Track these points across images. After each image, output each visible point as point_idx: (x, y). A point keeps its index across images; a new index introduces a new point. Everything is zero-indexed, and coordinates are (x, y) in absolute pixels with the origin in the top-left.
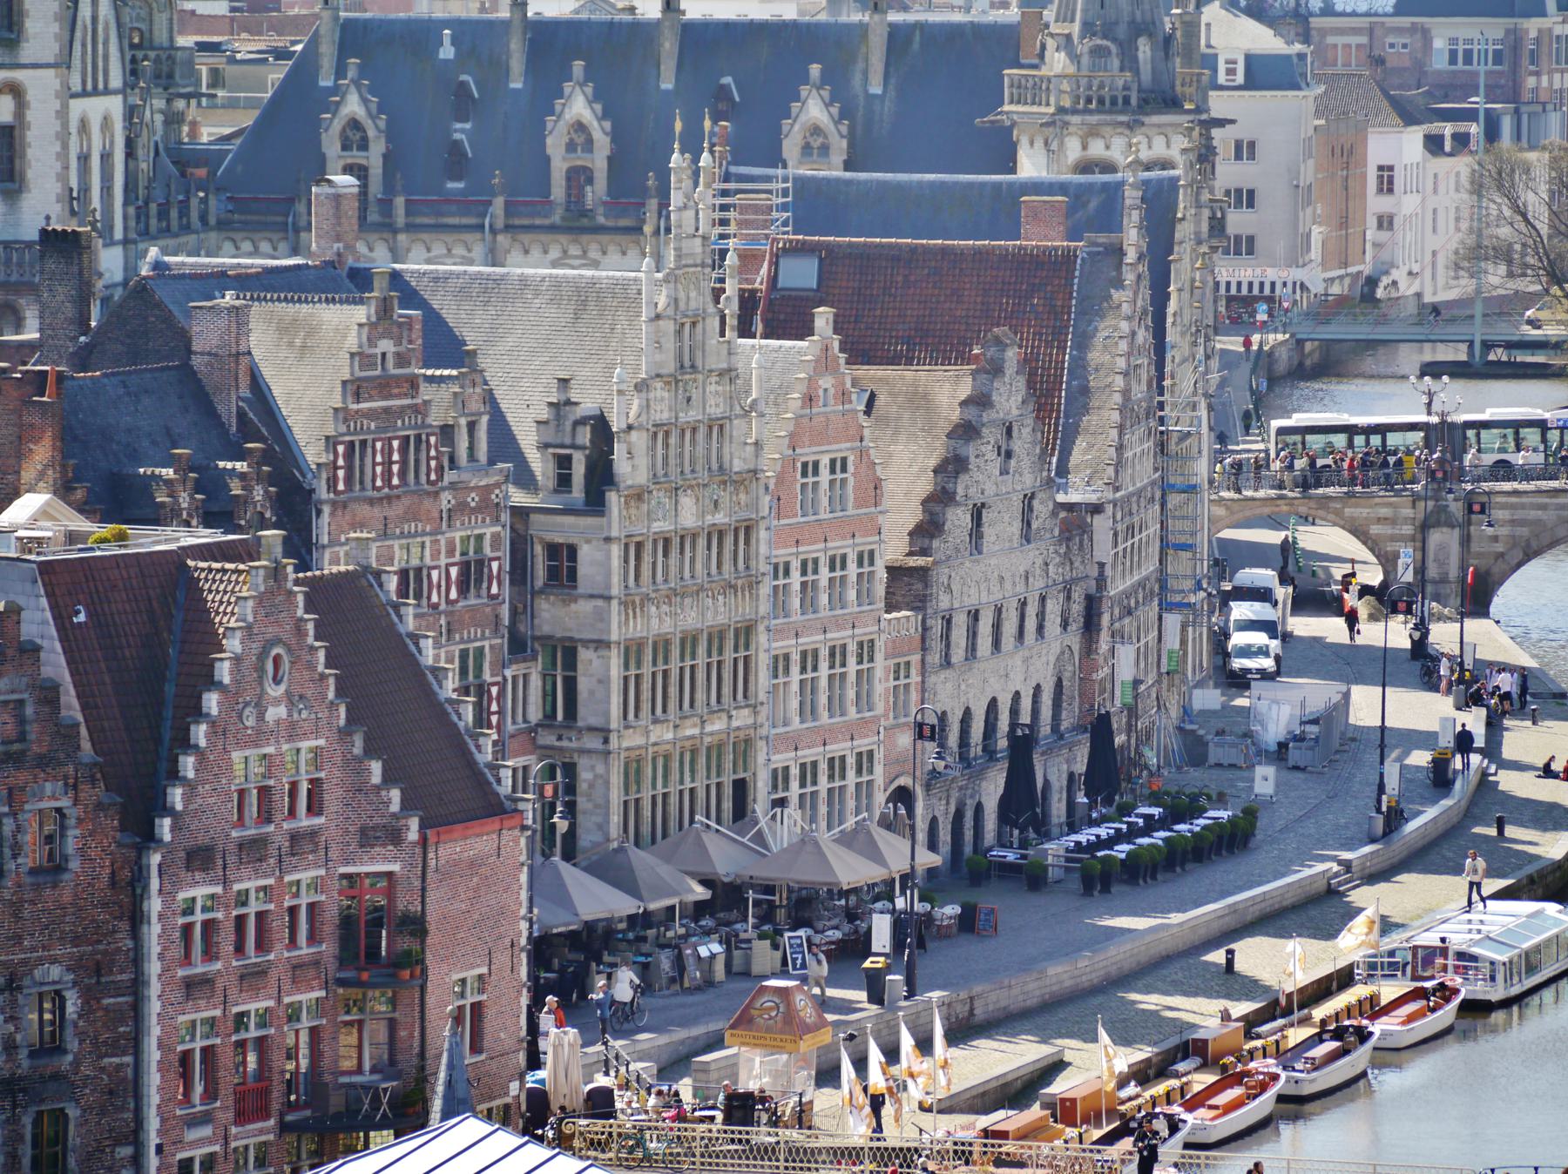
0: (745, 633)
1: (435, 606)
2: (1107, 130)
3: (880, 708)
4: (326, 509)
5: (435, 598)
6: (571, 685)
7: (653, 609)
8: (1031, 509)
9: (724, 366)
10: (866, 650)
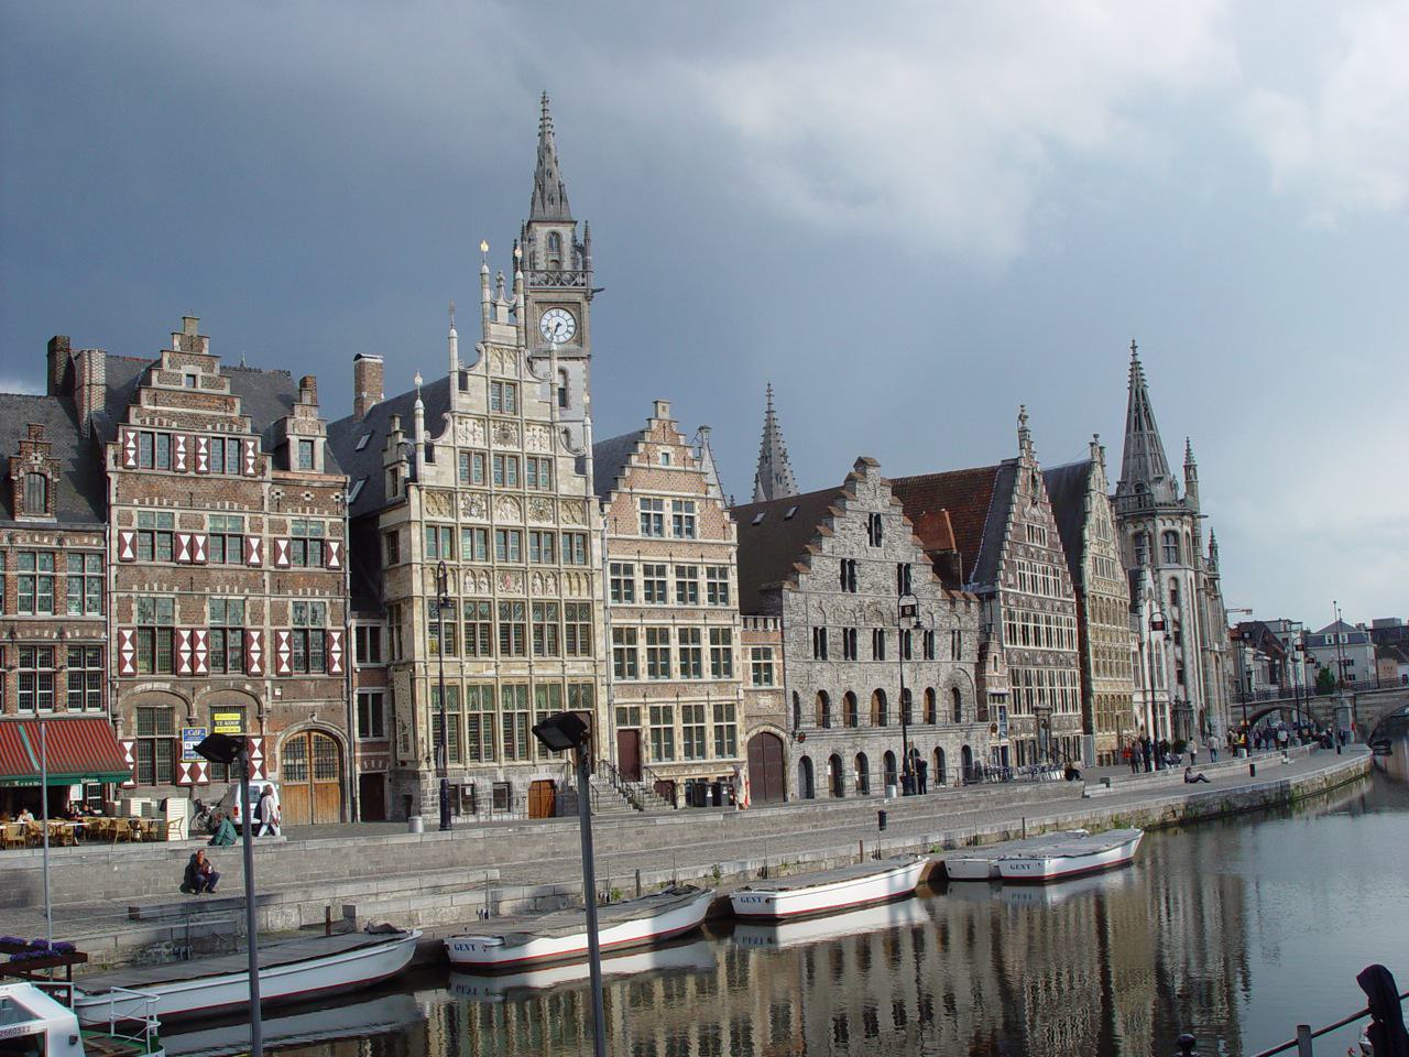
0: (582, 610)
1: (259, 565)
2: (1145, 519)
3: (738, 675)
4: (114, 478)
5: (254, 559)
6: (399, 628)
7: (469, 579)
8: (908, 575)
9: (549, 419)
10: (721, 635)
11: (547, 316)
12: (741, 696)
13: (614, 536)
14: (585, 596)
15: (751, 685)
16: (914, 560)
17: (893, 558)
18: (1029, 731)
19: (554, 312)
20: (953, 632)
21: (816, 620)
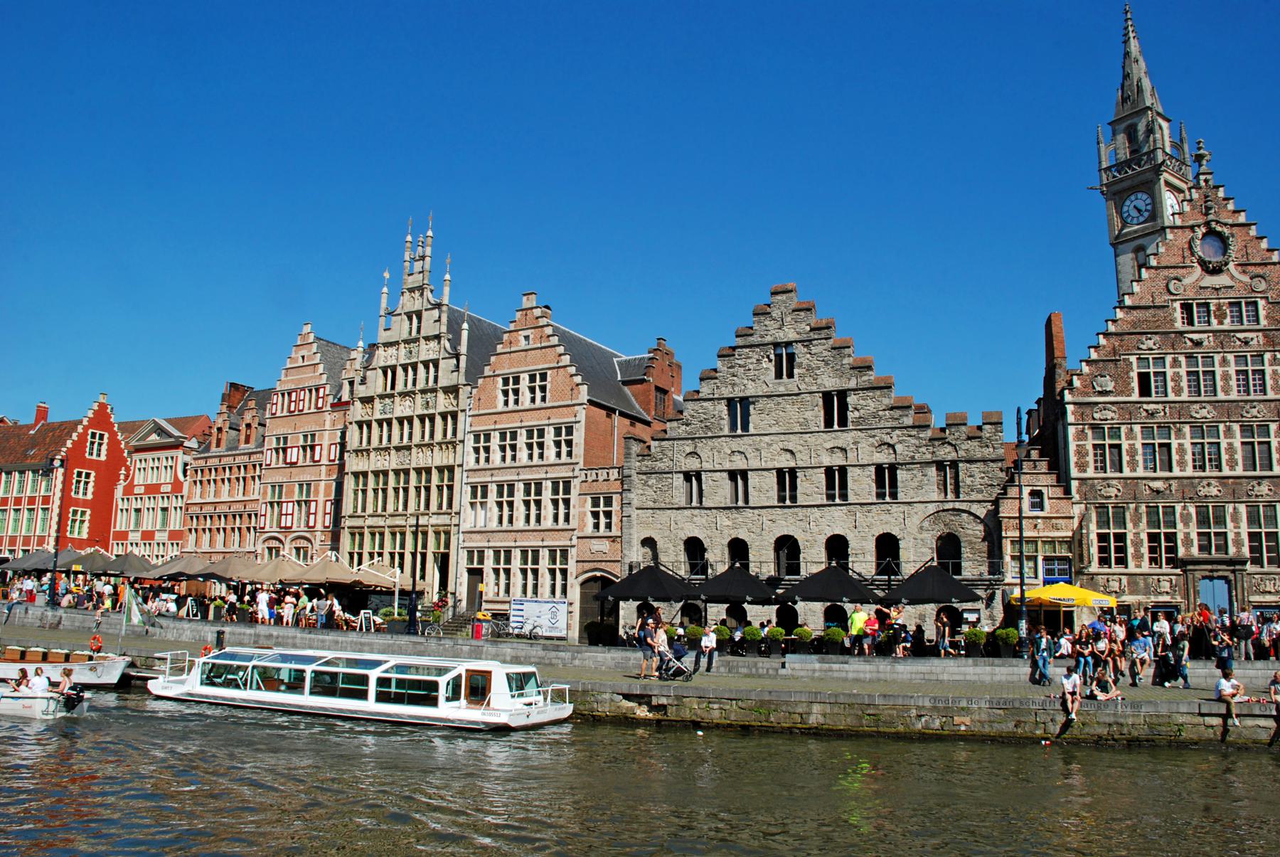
3: (574, 523)
8: (844, 407)
11: (1128, 203)
12: (575, 541)
13: (476, 412)
14: (451, 462)
15: (589, 530)
16: (852, 384)
17: (814, 388)
18: (1147, 592)
19: (1133, 197)
20: (940, 466)
21: (693, 464)
